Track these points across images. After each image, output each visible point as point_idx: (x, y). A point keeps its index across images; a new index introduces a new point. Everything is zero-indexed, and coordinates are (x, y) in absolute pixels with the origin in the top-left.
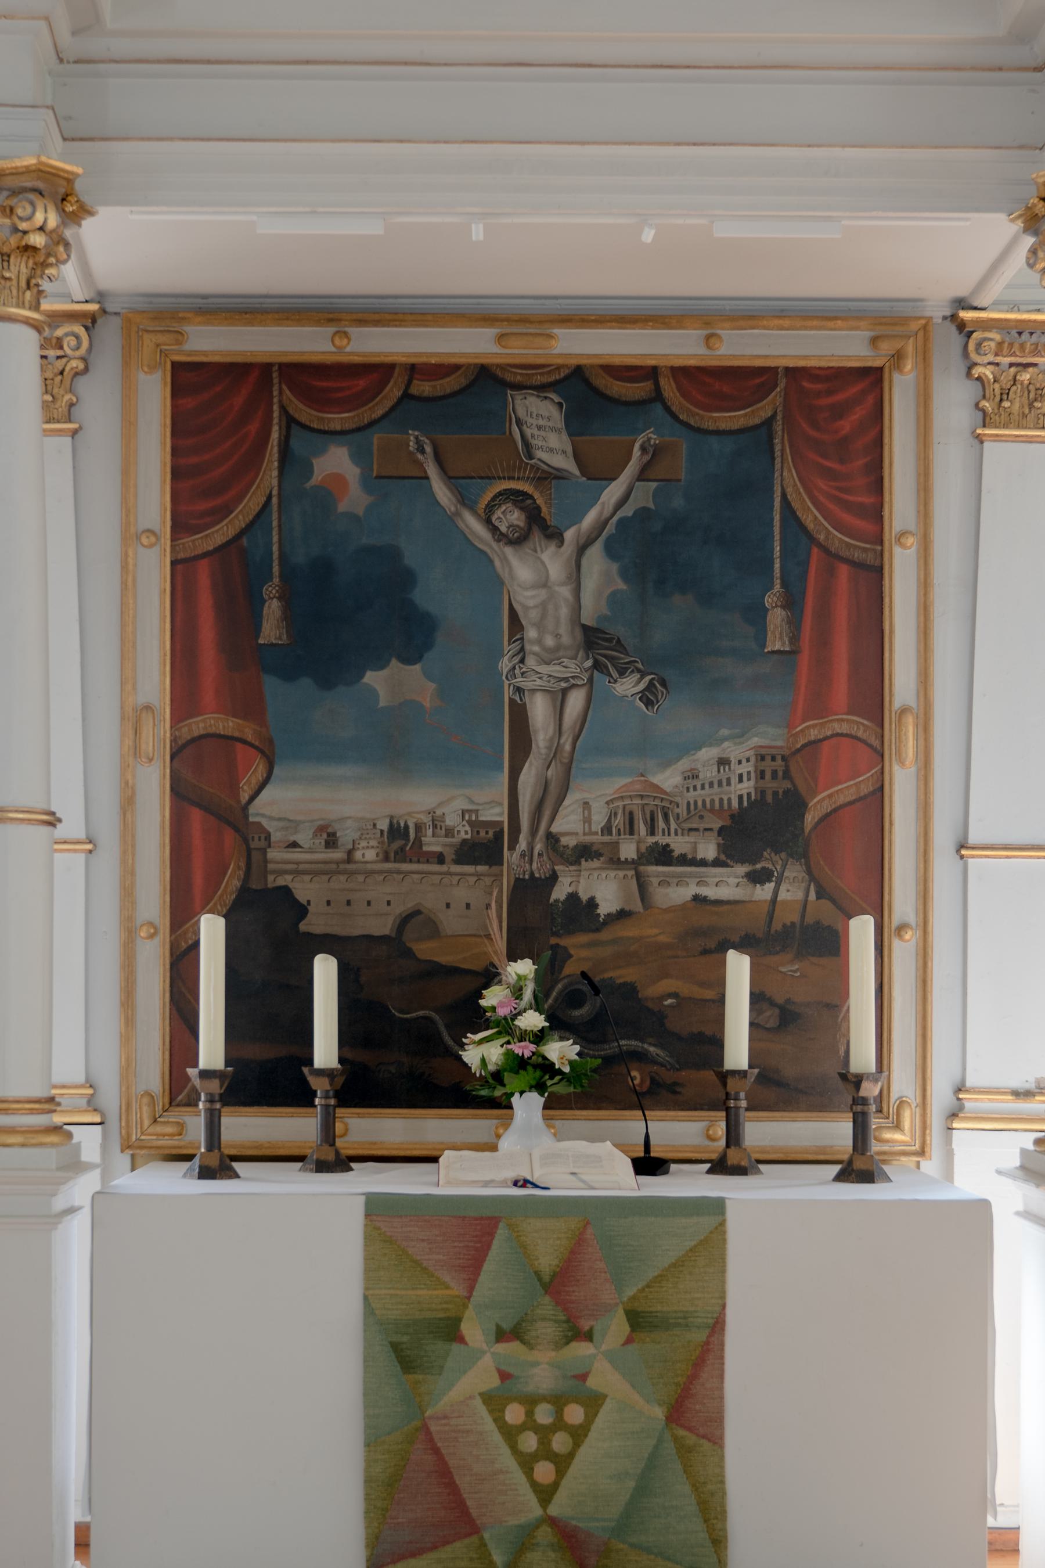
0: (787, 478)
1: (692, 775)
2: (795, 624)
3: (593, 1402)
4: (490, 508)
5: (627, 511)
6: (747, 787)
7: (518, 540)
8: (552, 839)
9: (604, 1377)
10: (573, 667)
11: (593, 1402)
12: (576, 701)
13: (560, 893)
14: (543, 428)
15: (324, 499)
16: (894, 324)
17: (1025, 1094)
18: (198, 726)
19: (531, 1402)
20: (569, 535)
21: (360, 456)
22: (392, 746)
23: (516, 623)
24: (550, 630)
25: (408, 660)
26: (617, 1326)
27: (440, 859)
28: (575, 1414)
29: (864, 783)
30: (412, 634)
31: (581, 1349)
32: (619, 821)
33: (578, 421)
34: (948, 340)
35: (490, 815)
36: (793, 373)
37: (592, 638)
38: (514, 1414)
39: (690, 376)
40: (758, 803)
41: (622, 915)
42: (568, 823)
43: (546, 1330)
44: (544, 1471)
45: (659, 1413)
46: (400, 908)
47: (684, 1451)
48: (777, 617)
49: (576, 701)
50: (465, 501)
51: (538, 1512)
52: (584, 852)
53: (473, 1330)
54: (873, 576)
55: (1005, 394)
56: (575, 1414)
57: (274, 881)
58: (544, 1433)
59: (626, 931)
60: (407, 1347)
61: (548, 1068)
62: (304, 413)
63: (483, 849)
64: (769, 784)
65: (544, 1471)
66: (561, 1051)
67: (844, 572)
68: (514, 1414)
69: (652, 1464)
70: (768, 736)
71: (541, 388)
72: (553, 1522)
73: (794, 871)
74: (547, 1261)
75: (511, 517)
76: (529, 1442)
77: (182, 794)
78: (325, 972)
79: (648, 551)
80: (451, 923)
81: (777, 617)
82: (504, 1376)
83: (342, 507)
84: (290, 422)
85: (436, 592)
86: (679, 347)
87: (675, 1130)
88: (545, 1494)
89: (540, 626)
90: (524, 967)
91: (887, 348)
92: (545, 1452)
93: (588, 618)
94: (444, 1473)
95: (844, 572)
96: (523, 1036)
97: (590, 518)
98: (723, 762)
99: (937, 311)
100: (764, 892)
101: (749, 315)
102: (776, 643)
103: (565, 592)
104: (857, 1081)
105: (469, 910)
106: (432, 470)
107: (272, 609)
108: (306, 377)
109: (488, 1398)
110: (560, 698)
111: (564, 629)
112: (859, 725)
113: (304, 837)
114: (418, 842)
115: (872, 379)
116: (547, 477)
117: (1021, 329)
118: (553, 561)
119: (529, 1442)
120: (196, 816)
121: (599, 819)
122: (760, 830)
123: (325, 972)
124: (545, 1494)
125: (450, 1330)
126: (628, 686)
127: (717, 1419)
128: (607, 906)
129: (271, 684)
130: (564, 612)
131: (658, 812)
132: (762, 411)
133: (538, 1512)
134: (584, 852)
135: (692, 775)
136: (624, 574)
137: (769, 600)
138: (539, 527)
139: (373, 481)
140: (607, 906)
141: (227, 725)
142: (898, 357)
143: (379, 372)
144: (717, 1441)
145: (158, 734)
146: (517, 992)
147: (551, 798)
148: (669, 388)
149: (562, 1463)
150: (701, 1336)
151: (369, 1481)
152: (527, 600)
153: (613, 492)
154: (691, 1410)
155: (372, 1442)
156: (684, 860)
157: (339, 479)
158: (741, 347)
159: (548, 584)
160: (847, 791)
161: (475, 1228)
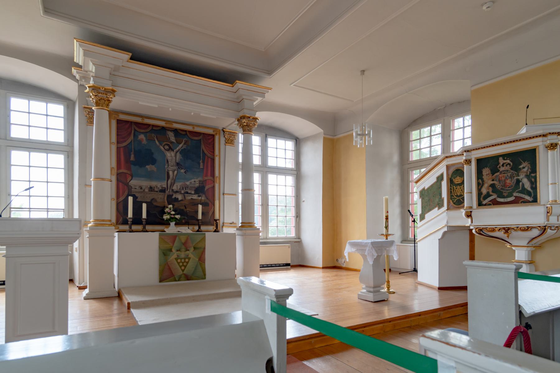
0: (203, 147)
1: (191, 183)
3: (189, 259)
5: (183, 148)
6: (198, 185)
7: (168, 150)
8: (173, 190)
9: (191, 255)
10: (175, 168)
11: (189, 259)
12: (176, 172)
13: (174, 197)
14: (172, 136)
15: (140, 141)
16: (215, 129)
17: (231, 224)
18: (121, 171)
19: (181, 259)
21: (145, 136)
22: (149, 176)
23: (168, 161)
24: (172, 162)
25: (153, 165)
26: (192, 249)
28: (187, 260)
29: (212, 185)
30: (153, 161)
31: (188, 252)
33: (176, 136)
34: (222, 133)
36: (203, 133)
37: (178, 164)
38: (179, 261)
39: (191, 132)
40: (199, 187)
41: (182, 200)
42: (175, 188)
43: (183, 250)
44: (183, 268)
45: (197, 260)
46: (151, 198)
47: (201, 264)
48: (201, 164)
49: (176, 172)
50: (161, 144)
51: (181, 272)
52: (177, 192)
53: (174, 250)
54: (213, 160)
56: (187, 260)
58: (183, 263)
59: (182, 202)
60: (165, 253)
61: (176, 219)
62: (137, 129)
63: (163, 191)
65: (183, 268)
66: (178, 217)
67: (210, 159)
68: (179, 261)
69: (197, 266)
70: (200, 179)
71: (171, 131)
72: (184, 274)
73: (204, 196)
74: (183, 241)
75: (167, 147)
76: (181, 264)
77: (118, 180)
78: (144, 206)
80: (159, 200)
81: (201, 164)
82: (178, 256)
84: (135, 130)
85: (156, 156)
86: (190, 128)
88: (183, 270)
90: (171, 206)
91: (215, 132)
92: (183, 265)
93: (177, 161)
94: (170, 269)
96: (171, 215)
97: (178, 149)
99: (221, 129)
100: (200, 198)
101: (198, 126)
102: (201, 167)
103: (174, 158)
104: (216, 220)
105: (161, 199)
108: (137, 124)
109: (175, 259)
110: (174, 172)
112: (211, 178)
113: (137, 188)
115: (213, 136)
116: (172, 143)
117: (231, 132)
118: (173, 154)
119: (181, 264)
120: (121, 184)
121: (179, 188)
122: (199, 190)
123: (144, 206)
124: (183, 270)
125: (171, 250)
126: (183, 171)
127: (205, 260)
128: (180, 199)
129: (132, 167)
131: (187, 187)
133: (181, 272)
134: (177, 192)
135: (191, 183)
136: (182, 156)
138: (171, 149)
139: (148, 140)
140: (180, 199)
142: (216, 134)
143: (149, 125)
144: (204, 263)
145: (115, 171)
146: (170, 209)
147: (172, 184)
149: (185, 267)
150: (202, 250)
151: (160, 270)
152: (169, 158)
153: (181, 146)
154: (201, 259)
155: (160, 265)
157: (143, 139)
160: (210, 186)
161: (174, 237)
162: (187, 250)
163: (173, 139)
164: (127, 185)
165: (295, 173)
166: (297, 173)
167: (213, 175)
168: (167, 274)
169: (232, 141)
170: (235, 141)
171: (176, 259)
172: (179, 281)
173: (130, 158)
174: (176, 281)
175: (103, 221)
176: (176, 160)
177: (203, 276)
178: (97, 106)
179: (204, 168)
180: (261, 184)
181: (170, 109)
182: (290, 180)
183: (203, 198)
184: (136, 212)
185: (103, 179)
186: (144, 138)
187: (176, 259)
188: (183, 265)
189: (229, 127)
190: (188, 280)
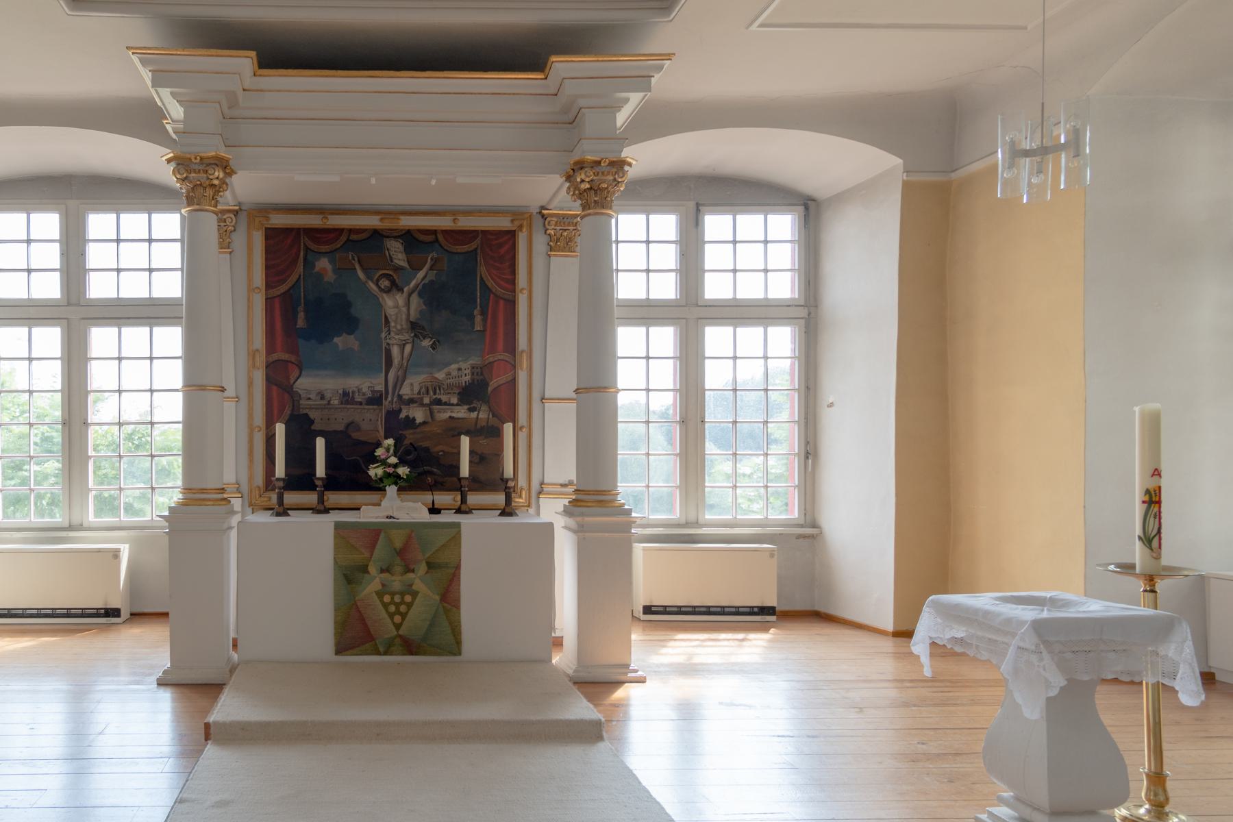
0: (482, 270)
1: (449, 374)
2: (485, 321)
3: (415, 594)
4: (378, 280)
5: (426, 281)
6: (468, 378)
7: (388, 291)
8: (400, 397)
9: (419, 585)
10: (407, 336)
11: (415, 594)
12: (408, 348)
13: (402, 415)
14: (397, 252)
16: (521, 216)
18: (275, 357)
19: (393, 594)
20: (406, 289)
21: (332, 262)
22: (343, 364)
26: (422, 568)
27: (361, 403)
28: (408, 598)
29: (508, 377)
30: (350, 324)
31: (411, 575)
32: (423, 390)
34: (538, 222)
35: (378, 388)
37: (414, 326)
38: (387, 599)
39: (447, 233)
41: (424, 423)
42: (406, 391)
43: (398, 569)
44: (397, 619)
45: (438, 598)
48: (478, 319)
49: (408, 348)
50: (370, 278)
53: (373, 569)
54: (512, 304)
55: (558, 240)
57: (303, 412)
58: (397, 605)
59: (426, 429)
60: (349, 575)
62: (312, 246)
63: (375, 400)
64: (476, 377)
65: (397, 619)
66: (403, 471)
67: (502, 302)
68: (387, 599)
70: (475, 360)
71: (395, 237)
72: (400, 636)
73: (484, 408)
74: (398, 544)
75: (385, 283)
76: (392, 608)
77: (269, 380)
78: (320, 443)
79: (433, 295)
80: (365, 426)
81: (478, 319)
82: (383, 585)
83: (326, 279)
84: (307, 249)
86: (444, 223)
87: (443, 498)
89: (396, 322)
90: (390, 441)
91: (517, 223)
92: (398, 612)
94: (362, 620)
95: (502, 302)
96: (390, 466)
98: (460, 369)
99: (535, 210)
100: (474, 415)
101: (469, 212)
102: (478, 327)
103: (404, 309)
104: (507, 480)
105: (371, 422)
106: (357, 266)
107: (301, 315)
108: (311, 232)
109: (378, 593)
110: (402, 347)
111: (404, 323)
112: (505, 356)
114: (353, 398)
115: (511, 235)
116: (398, 269)
117: (564, 216)
118: (400, 299)
120: (275, 388)
121: (416, 389)
122: (472, 393)
123: (320, 443)
125: (364, 569)
126: (426, 343)
127: (458, 600)
128: (419, 419)
129: (301, 342)
130: (404, 317)
131: (437, 386)
132: (473, 246)
134: (411, 401)
135: (449, 374)
137: (476, 312)
138: (395, 287)
139: (336, 270)
140: (419, 419)
141: (285, 356)
142: (521, 227)
143: (339, 231)
144: (458, 607)
145: (261, 359)
146: (388, 450)
147: (399, 382)
148: (440, 238)
149: (404, 616)
150: (451, 571)
153: (421, 274)
154: (449, 597)
155: (337, 609)
156: (446, 404)
158: (466, 223)
159: (398, 307)
161: (373, 533)
162: (409, 570)
163: (400, 258)
164: (288, 390)
165: (803, 312)
166: (808, 314)
167: (511, 346)
168: (354, 634)
169: (569, 240)
170: (578, 239)
171: (380, 594)
172: (386, 653)
173: (296, 323)
174: (378, 653)
175: (203, 491)
176: (408, 315)
177: (453, 646)
178: (189, 205)
179: (484, 331)
180: (680, 358)
181: (373, 181)
182: (783, 339)
183: (483, 414)
184: (318, 459)
185: (202, 388)
186: (329, 267)
187: (380, 594)
188: (398, 612)
189: (555, 203)
190: (411, 653)
